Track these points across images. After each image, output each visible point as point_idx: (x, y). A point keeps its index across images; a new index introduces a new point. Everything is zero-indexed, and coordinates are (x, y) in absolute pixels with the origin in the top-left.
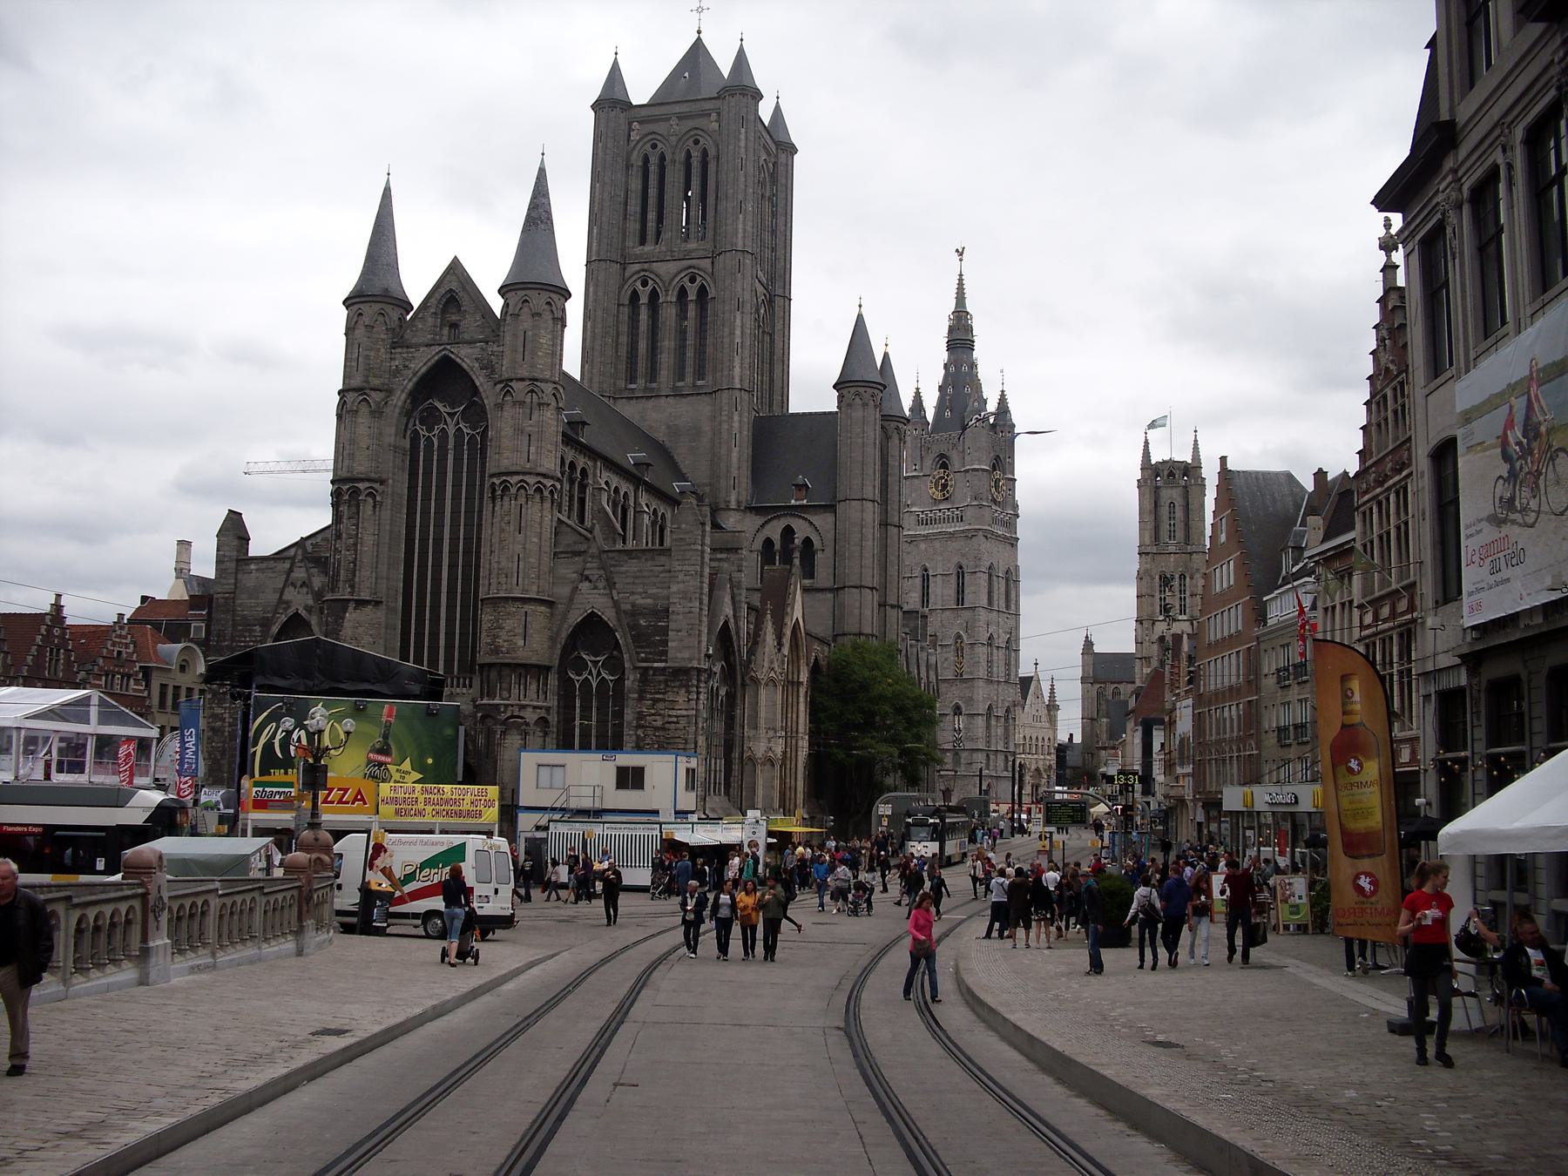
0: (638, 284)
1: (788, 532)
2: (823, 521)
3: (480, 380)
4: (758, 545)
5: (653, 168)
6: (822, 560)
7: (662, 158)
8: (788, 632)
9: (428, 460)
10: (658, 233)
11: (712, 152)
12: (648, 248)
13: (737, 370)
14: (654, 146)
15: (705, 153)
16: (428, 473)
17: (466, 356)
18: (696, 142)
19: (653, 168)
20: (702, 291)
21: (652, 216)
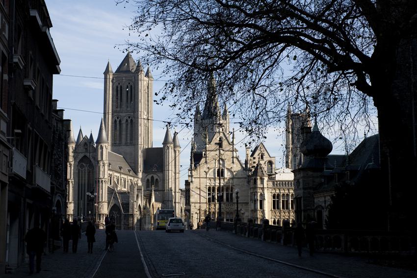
0: (116, 118)
1: (152, 177)
2: (160, 175)
3: (92, 160)
4: (146, 179)
5: (119, 89)
6: (160, 183)
7: (121, 87)
8: (151, 205)
9: (82, 175)
10: (121, 104)
11: (133, 86)
12: (118, 109)
13: (140, 141)
14: (119, 84)
15: (131, 86)
16: (82, 177)
17: (88, 155)
18: (129, 83)
19: (119, 89)
20: (131, 120)
21: (119, 101)
